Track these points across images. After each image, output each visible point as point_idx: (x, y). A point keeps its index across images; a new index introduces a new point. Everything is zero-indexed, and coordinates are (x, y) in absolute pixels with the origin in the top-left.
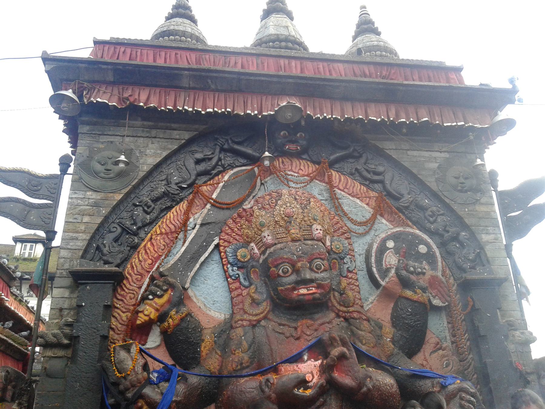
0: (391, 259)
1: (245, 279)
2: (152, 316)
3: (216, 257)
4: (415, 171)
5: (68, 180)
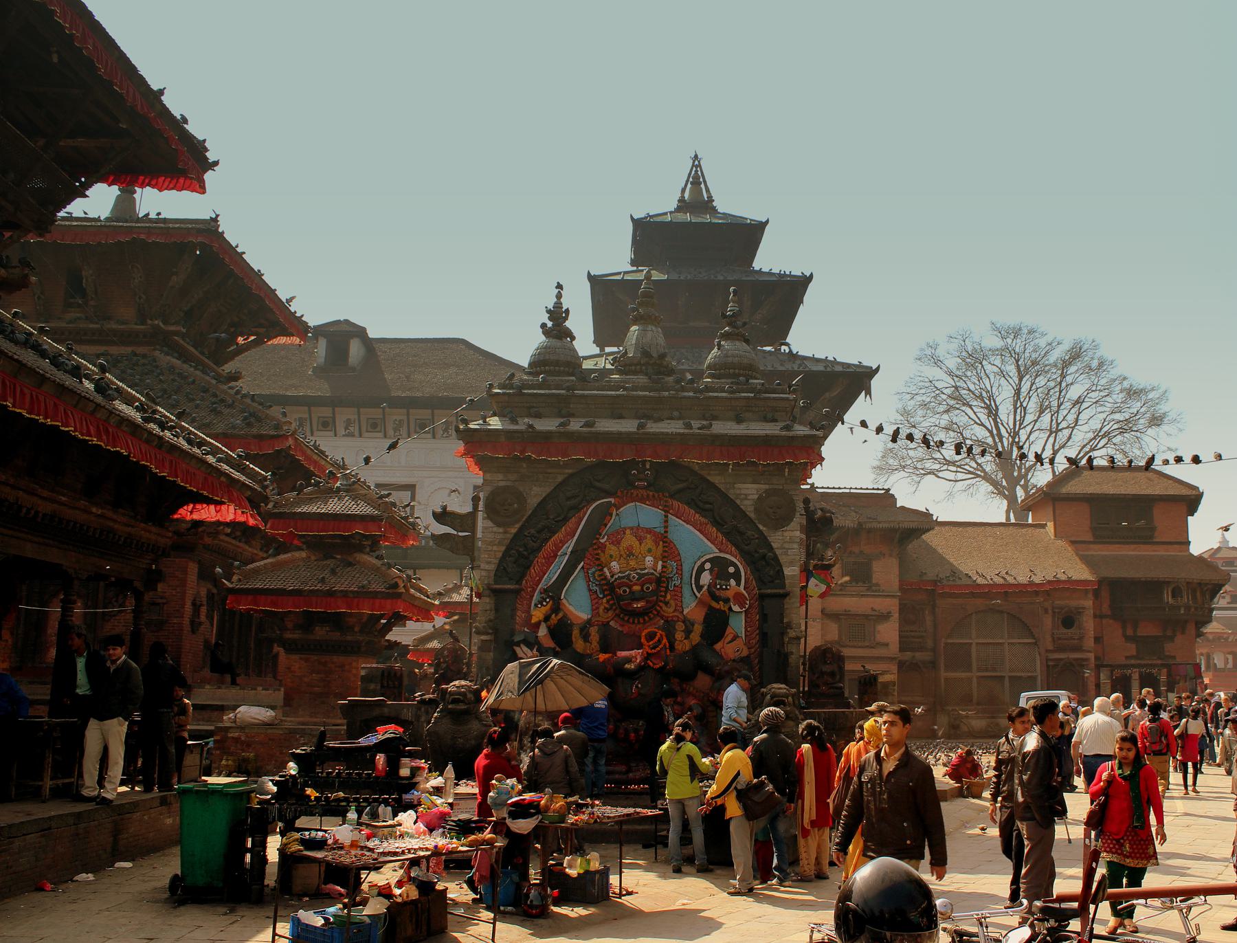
0: (706, 578)
3: (582, 574)
4: (738, 502)
5: (480, 515)
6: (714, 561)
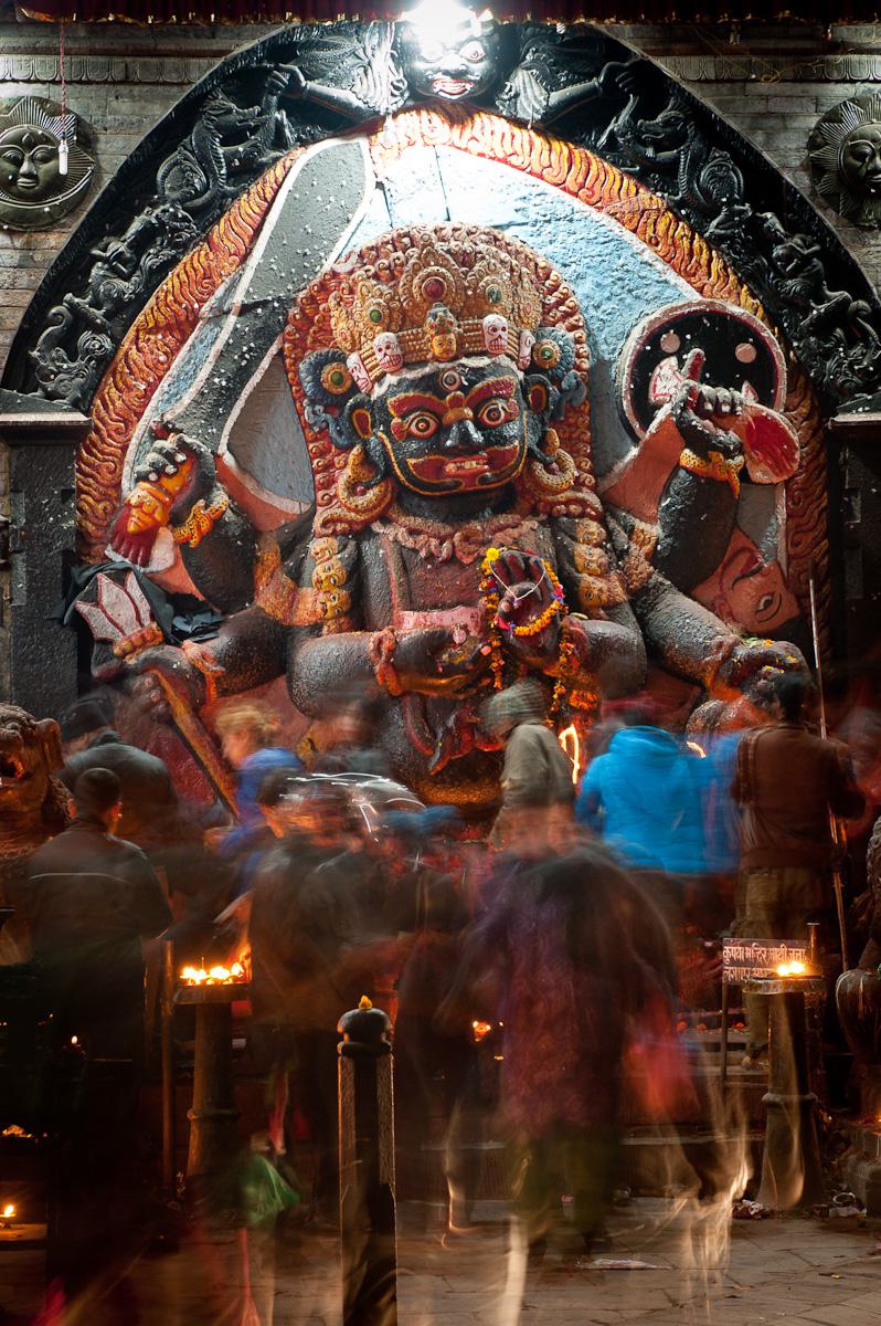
1: (340, 433)
2: (157, 516)
6: (686, 325)
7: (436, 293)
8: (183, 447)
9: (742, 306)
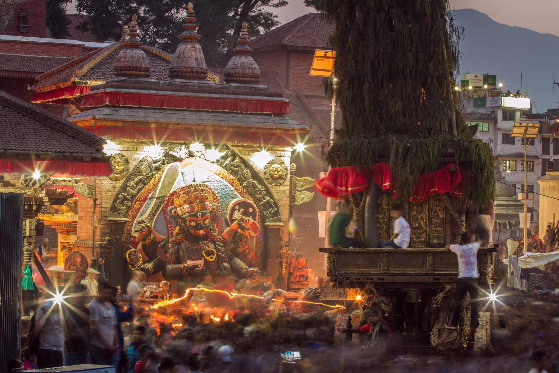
6: (241, 204)
7: (196, 198)
8: (146, 225)
9: (250, 201)
